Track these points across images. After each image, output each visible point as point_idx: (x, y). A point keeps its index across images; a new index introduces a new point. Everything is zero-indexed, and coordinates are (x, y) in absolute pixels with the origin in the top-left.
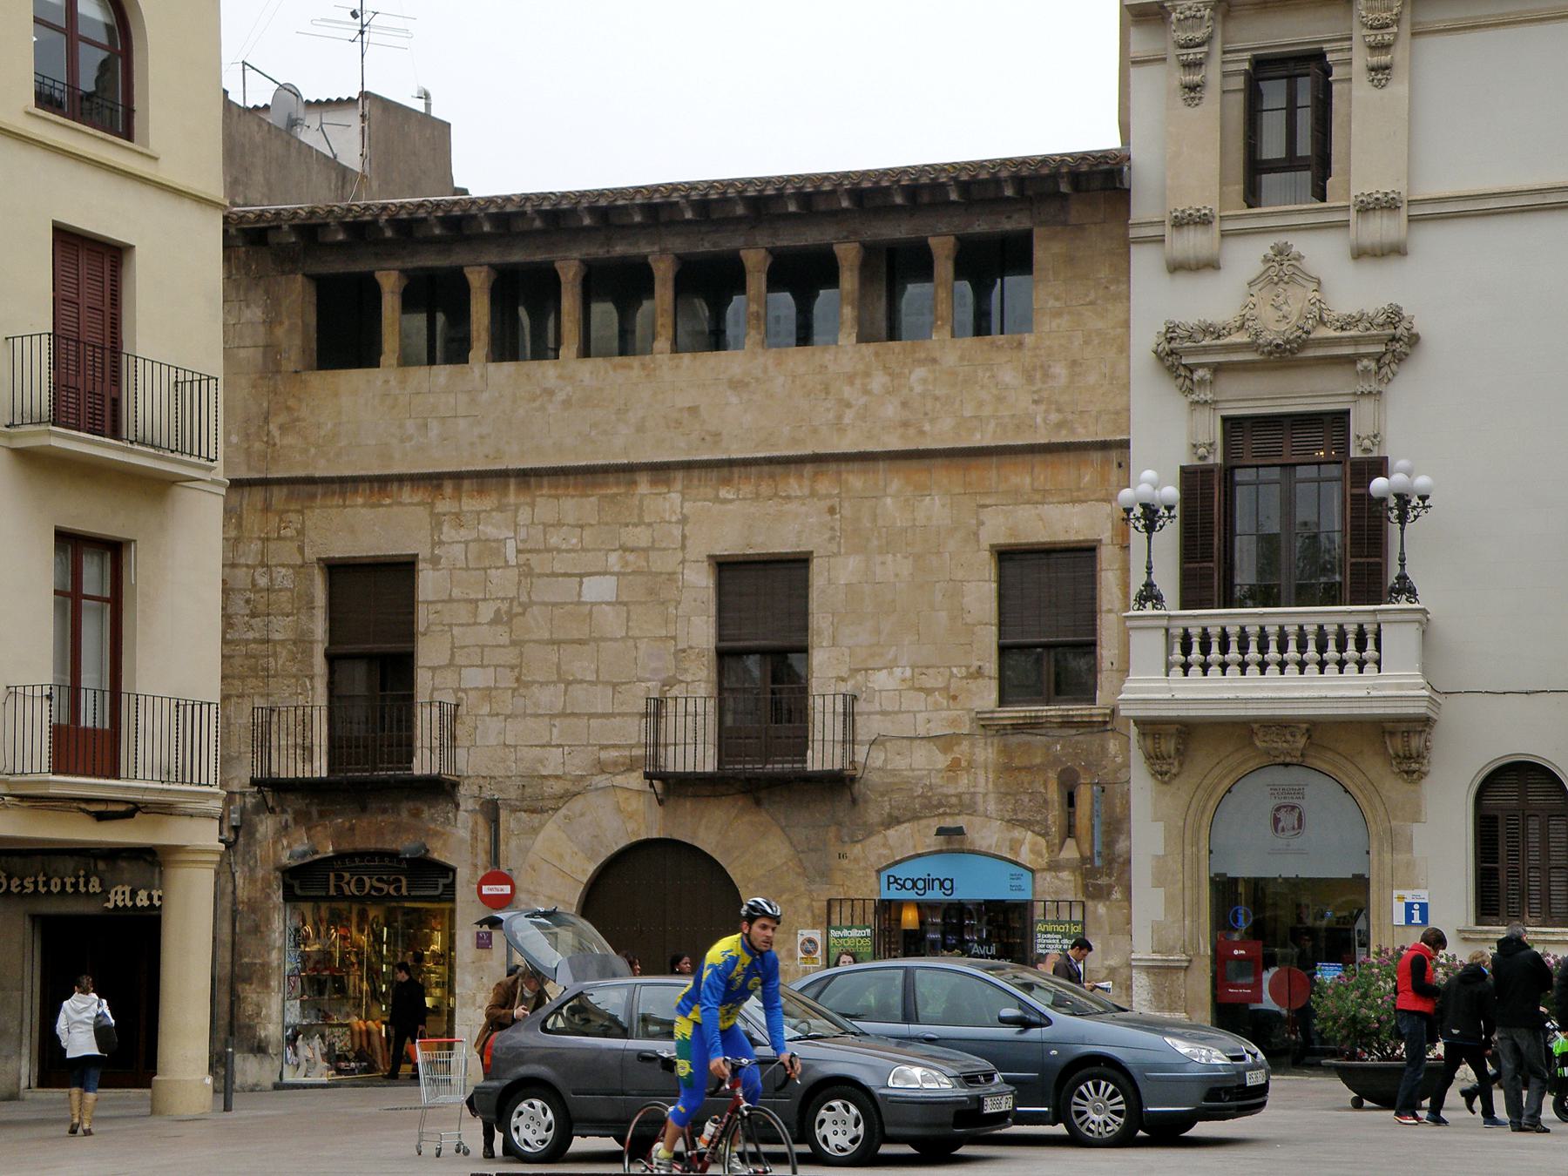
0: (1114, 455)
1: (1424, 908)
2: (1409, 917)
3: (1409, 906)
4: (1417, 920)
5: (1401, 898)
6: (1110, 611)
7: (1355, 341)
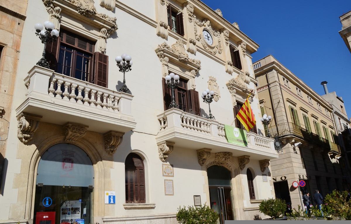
0: (18, 20)
1: (114, 197)
2: (110, 201)
3: (110, 197)
4: (112, 202)
5: (107, 194)
6: (7, 71)
7: (105, 22)
